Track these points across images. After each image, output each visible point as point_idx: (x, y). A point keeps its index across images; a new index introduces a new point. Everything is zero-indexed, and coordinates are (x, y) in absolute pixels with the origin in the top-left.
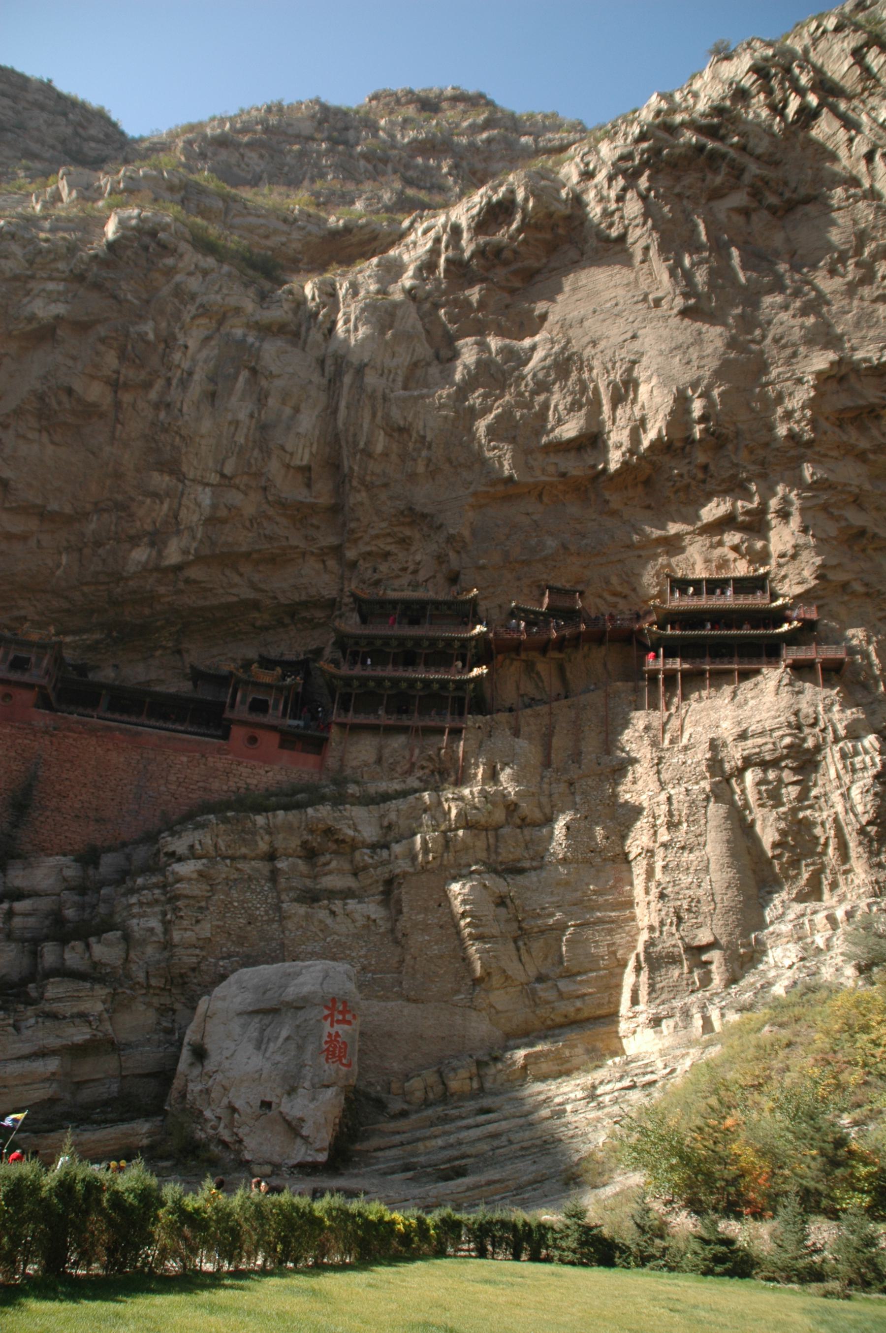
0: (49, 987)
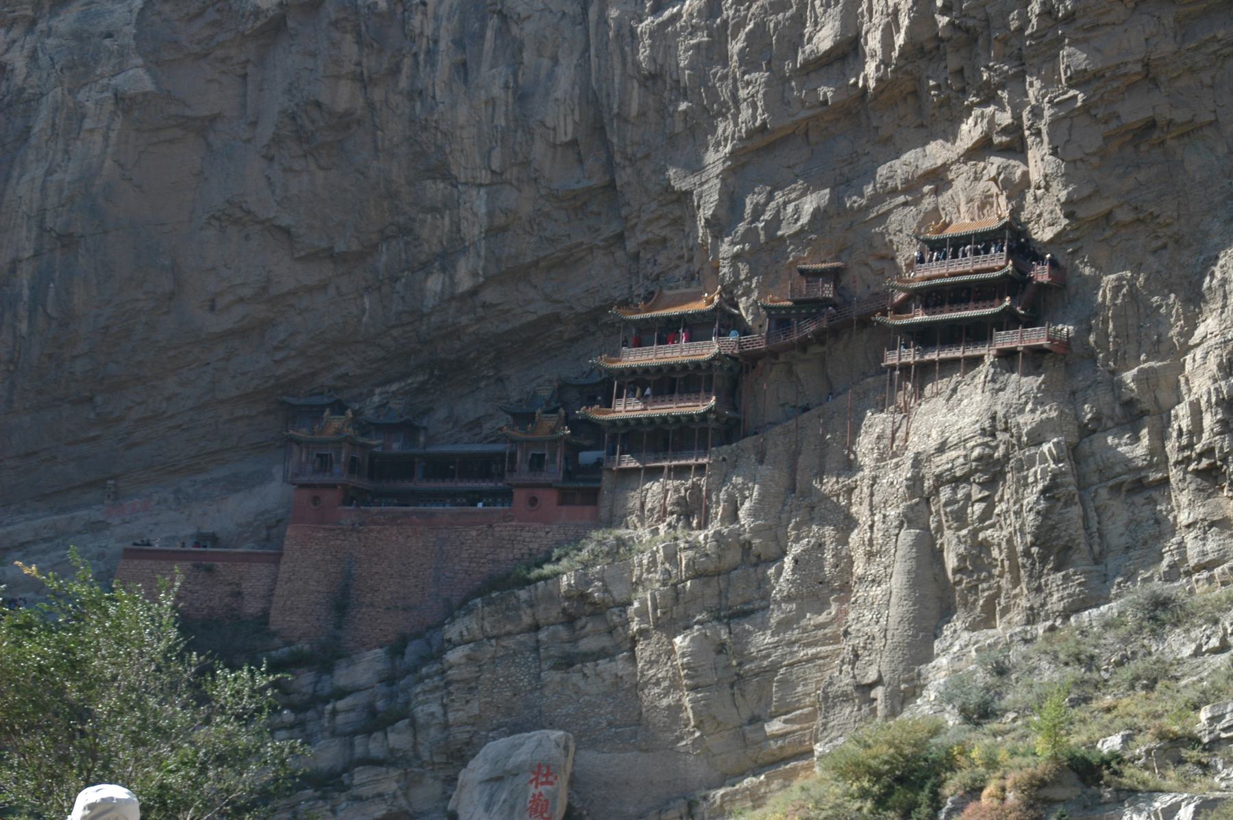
0: (356, 776)
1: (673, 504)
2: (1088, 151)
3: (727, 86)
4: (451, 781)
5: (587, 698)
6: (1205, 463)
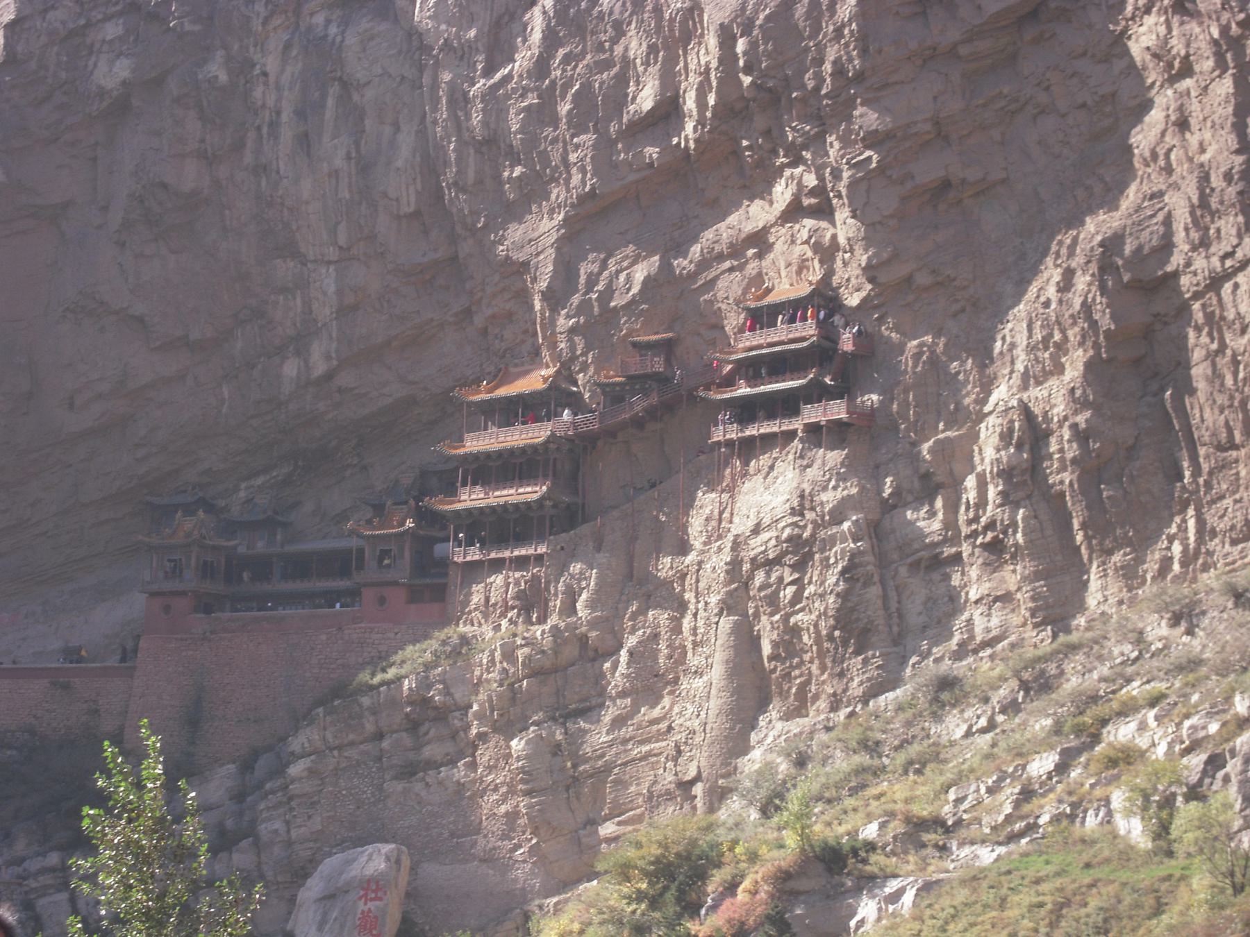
1: (513, 598)
2: (886, 213)
3: (557, 150)
4: (292, 900)
5: (430, 808)
6: (990, 535)
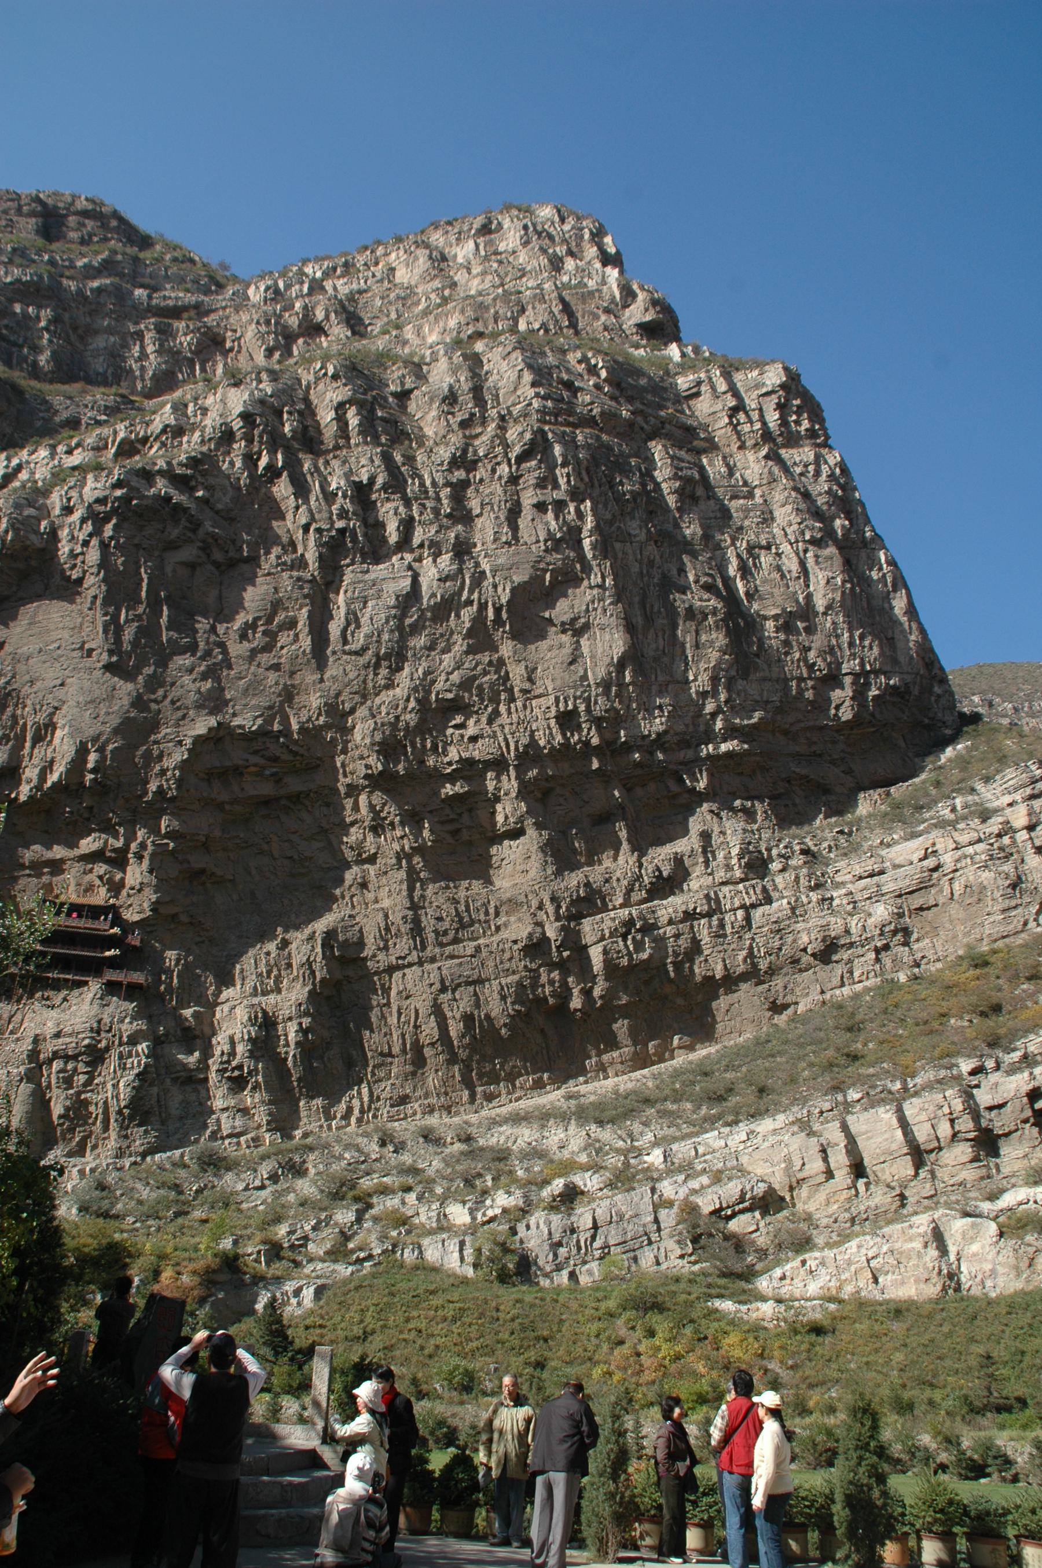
6: (236, 1073)
